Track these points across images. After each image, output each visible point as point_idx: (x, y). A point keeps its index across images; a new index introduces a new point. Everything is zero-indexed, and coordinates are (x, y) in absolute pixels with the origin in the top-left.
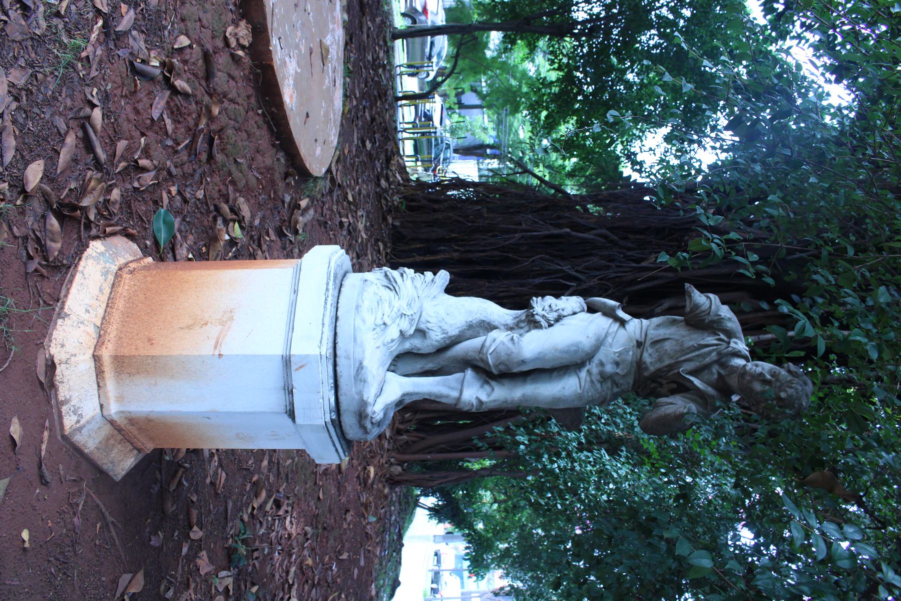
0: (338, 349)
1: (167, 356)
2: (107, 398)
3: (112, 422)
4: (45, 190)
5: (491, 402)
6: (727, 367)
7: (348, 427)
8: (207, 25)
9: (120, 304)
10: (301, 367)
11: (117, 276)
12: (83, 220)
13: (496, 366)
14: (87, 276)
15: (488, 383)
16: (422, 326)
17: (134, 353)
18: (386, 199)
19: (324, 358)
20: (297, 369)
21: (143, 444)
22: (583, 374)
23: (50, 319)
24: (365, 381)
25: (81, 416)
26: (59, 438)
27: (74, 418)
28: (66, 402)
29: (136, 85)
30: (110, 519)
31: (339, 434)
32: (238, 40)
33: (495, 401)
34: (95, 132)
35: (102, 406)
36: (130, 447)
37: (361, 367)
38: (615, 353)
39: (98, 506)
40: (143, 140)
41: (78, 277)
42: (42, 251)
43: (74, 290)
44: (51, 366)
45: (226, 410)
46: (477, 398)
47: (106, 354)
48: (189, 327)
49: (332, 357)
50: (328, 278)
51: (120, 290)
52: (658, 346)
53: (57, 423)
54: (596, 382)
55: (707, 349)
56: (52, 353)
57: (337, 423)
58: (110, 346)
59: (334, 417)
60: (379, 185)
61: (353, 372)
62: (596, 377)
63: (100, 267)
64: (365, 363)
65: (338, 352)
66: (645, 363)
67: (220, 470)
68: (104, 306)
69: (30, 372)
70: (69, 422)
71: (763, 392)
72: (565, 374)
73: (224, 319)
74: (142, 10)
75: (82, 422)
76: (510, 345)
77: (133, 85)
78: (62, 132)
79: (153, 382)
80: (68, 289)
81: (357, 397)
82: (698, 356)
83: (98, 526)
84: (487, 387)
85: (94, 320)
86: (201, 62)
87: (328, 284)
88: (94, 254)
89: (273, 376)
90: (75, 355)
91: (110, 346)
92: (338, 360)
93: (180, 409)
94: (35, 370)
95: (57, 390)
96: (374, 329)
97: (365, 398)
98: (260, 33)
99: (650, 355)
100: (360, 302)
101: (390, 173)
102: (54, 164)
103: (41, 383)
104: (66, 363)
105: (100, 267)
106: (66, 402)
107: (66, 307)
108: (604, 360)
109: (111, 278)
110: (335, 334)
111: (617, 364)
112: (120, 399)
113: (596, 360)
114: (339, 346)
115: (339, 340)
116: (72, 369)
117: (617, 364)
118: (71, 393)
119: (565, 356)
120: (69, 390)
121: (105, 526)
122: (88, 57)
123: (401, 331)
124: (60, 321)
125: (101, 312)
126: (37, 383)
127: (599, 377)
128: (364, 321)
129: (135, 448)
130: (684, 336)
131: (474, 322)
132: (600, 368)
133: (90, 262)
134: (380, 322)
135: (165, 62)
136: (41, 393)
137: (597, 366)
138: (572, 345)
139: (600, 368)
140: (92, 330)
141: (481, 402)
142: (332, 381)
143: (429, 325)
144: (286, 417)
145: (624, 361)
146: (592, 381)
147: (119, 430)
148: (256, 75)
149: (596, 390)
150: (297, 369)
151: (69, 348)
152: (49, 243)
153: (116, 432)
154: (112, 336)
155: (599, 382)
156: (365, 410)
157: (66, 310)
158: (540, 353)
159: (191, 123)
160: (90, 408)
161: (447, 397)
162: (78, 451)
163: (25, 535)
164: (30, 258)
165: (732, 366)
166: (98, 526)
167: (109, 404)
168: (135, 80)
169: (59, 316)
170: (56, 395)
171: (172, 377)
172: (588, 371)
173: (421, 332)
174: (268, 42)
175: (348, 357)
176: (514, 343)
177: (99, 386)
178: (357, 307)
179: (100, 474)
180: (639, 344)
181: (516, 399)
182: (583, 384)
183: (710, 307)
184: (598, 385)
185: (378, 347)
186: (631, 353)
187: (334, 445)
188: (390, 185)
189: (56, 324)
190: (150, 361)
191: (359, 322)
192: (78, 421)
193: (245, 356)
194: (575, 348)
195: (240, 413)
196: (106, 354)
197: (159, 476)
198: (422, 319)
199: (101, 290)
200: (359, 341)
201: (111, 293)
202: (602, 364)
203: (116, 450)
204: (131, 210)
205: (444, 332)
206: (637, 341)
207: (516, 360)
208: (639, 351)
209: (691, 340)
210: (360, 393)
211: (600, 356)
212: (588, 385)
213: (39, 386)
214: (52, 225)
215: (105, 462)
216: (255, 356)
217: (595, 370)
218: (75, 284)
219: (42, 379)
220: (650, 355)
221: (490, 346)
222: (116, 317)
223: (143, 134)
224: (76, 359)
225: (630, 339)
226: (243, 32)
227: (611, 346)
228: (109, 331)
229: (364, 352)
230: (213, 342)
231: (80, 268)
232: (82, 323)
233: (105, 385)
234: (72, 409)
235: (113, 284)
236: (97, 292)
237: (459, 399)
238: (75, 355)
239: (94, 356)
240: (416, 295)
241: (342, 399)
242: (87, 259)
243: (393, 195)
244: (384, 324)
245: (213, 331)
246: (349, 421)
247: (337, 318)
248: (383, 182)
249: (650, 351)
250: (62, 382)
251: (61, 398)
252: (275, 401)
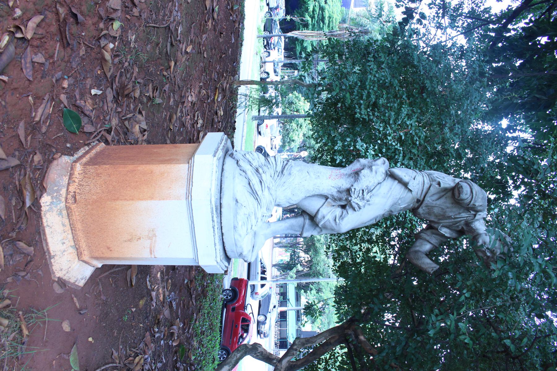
6: (469, 226)
9: (79, 226)
11: (68, 208)
14: (51, 225)
41: (47, 230)
48: (130, 241)
50: (212, 213)
51: (74, 218)
55: (459, 219)
58: (86, 252)
63: (55, 212)
65: (226, 250)
68: (70, 231)
73: (150, 235)
76: (333, 224)
87: (213, 217)
88: (47, 208)
91: (86, 252)
100: (236, 224)
105: (55, 212)
107: (51, 252)
109: (65, 212)
110: (223, 242)
114: (226, 248)
124: (52, 260)
125: (70, 236)
128: (240, 236)
130: (448, 208)
133: (48, 215)
140: (72, 250)
151: (65, 267)
154: (84, 246)
163: (90, 339)
165: (472, 227)
176: (336, 224)
178: (235, 227)
180: (418, 201)
183: (470, 202)
189: (51, 263)
191: (237, 237)
199: (64, 225)
201: (70, 221)
209: (451, 212)
221: (321, 220)
222: (80, 234)
225: (413, 199)
228: (81, 245)
230: (149, 250)
231: (45, 224)
232: (64, 251)
235: (68, 214)
236: (62, 228)
240: (272, 199)
247: (222, 234)
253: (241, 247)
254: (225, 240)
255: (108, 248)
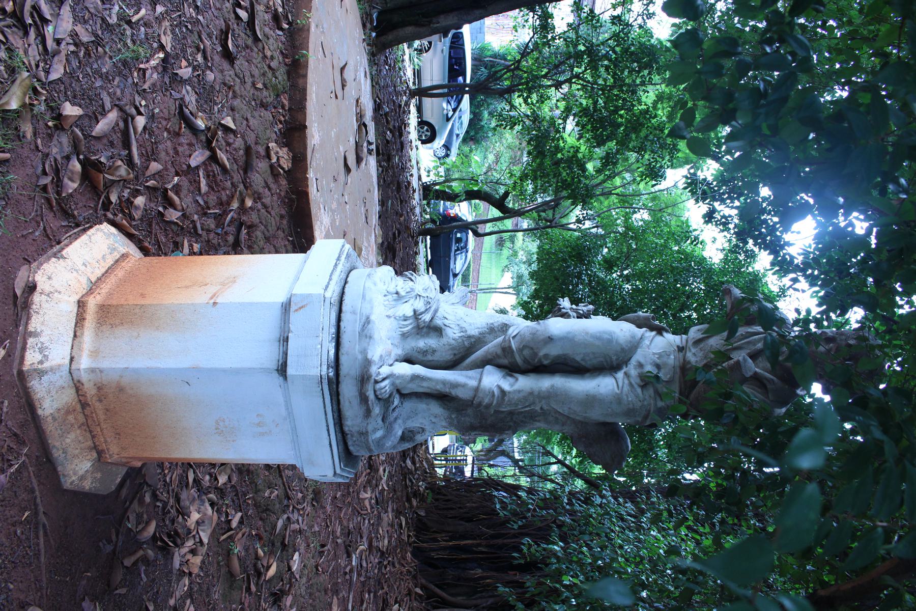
0: (344, 305)
1: (157, 305)
2: (81, 349)
3: (78, 386)
4: (77, 135)
5: (515, 391)
7: (347, 404)
8: (252, 128)
10: (300, 308)
12: (103, 197)
13: (521, 350)
15: (511, 376)
16: (438, 322)
17: (122, 302)
18: (410, 480)
19: (328, 302)
20: (296, 310)
21: (106, 442)
22: (620, 375)
23: (44, 251)
24: (370, 337)
25: (46, 357)
26: (15, 372)
27: (39, 357)
28: (35, 334)
29: (180, 128)
30: (43, 518)
31: (336, 415)
32: (278, 159)
33: (519, 391)
34: (135, 133)
35: (72, 359)
36: (90, 443)
37: (368, 321)
38: (654, 354)
39: (32, 491)
40: (176, 179)
42: (58, 186)
43: (77, 244)
44: (32, 288)
45: (209, 366)
46: (499, 387)
47: (92, 303)
48: (187, 287)
49: (337, 304)
51: (123, 264)
52: (702, 345)
53: (18, 353)
54: (636, 386)
56: (36, 279)
57: (334, 384)
59: (331, 374)
60: (404, 462)
61: (358, 328)
62: (635, 380)
64: (373, 318)
65: (344, 308)
66: (689, 362)
67: (188, 601)
69: (10, 276)
70: (32, 358)
71: (829, 351)
72: (599, 375)
74: (199, 75)
75: (46, 365)
77: (178, 126)
78: (107, 109)
79: (135, 334)
80: (71, 243)
81: (360, 357)
82: (748, 343)
83: (26, 514)
84: (511, 380)
85: (89, 274)
86: (241, 152)
89: (268, 328)
90: (60, 292)
92: (342, 315)
93: (159, 365)
94: (14, 280)
95: (29, 318)
96: (385, 296)
97: (369, 357)
98: (300, 161)
99: (694, 354)
101: (417, 459)
102: (91, 127)
103: (15, 296)
104: (48, 295)
106: (35, 334)
108: (642, 361)
111: (658, 366)
112: (95, 353)
113: (633, 362)
115: (346, 297)
116: (52, 304)
117: (658, 366)
118: (43, 328)
119: (597, 343)
120: (43, 323)
121: (33, 522)
122: (144, 70)
123: (415, 311)
125: (99, 273)
126: (11, 294)
127: (638, 381)
129: (95, 447)
131: (496, 325)
132: (639, 370)
133: (100, 234)
134: (392, 290)
135: (210, 127)
136: (11, 306)
137: (635, 368)
138: (605, 332)
139: (639, 370)
140: (84, 280)
141: (503, 392)
142: (333, 330)
143: (446, 322)
144: (276, 375)
145: (665, 364)
146: (631, 384)
147: (84, 405)
148: (291, 200)
149: (637, 396)
150: (296, 310)
151: (57, 283)
152: (66, 180)
153: (79, 407)
154: (103, 291)
155: (640, 386)
156: (368, 370)
157: (64, 253)
158: (569, 333)
159: (224, 198)
160: (59, 355)
161: (464, 386)
162: (29, 405)
164: (45, 173)
166: (26, 514)
167: (80, 356)
168: (180, 123)
169: (55, 255)
170: (27, 324)
171: (157, 329)
172: (625, 373)
173: (435, 330)
174: (305, 170)
175: (354, 313)
177: (75, 336)
179: (46, 463)
181: (544, 389)
182: (620, 384)
184: (639, 390)
185: (389, 317)
186: (672, 357)
187: (328, 430)
188: (416, 469)
190: (137, 311)
191: (369, 284)
192: (41, 362)
193: (241, 304)
194: (606, 336)
195: (224, 371)
196: (92, 303)
197: (114, 537)
198: (438, 314)
199: (104, 257)
200: (367, 298)
202: (640, 365)
203: (72, 436)
204: (151, 229)
205: (463, 330)
206: (678, 347)
207: (542, 337)
208: (681, 354)
210: (364, 352)
211: (638, 356)
212: (626, 388)
213: (12, 299)
214: (74, 166)
215: (57, 444)
216: (251, 304)
217: (633, 372)
218: (79, 241)
219: (19, 292)
220: (694, 354)
223: (177, 174)
224: (60, 296)
226: (283, 156)
227: (648, 347)
229: (372, 308)
232: (76, 270)
233: (82, 334)
234: (39, 345)
235: (117, 261)
236: (100, 257)
237: (477, 389)
238: (60, 292)
239: (79, 302)
241: (343, 359)
242: (98, 230)
243: (418, 480)
244: (397, 293)
245: (212, 290)
246: (348, 390)
247: (346, 282)
248: (409, 462)
249: (693, 350)
250: (38, 313)
251: (31, 328)
252: (267, 356)
253: (371, 301)
254: (346, 290)
255: (142, 295)
